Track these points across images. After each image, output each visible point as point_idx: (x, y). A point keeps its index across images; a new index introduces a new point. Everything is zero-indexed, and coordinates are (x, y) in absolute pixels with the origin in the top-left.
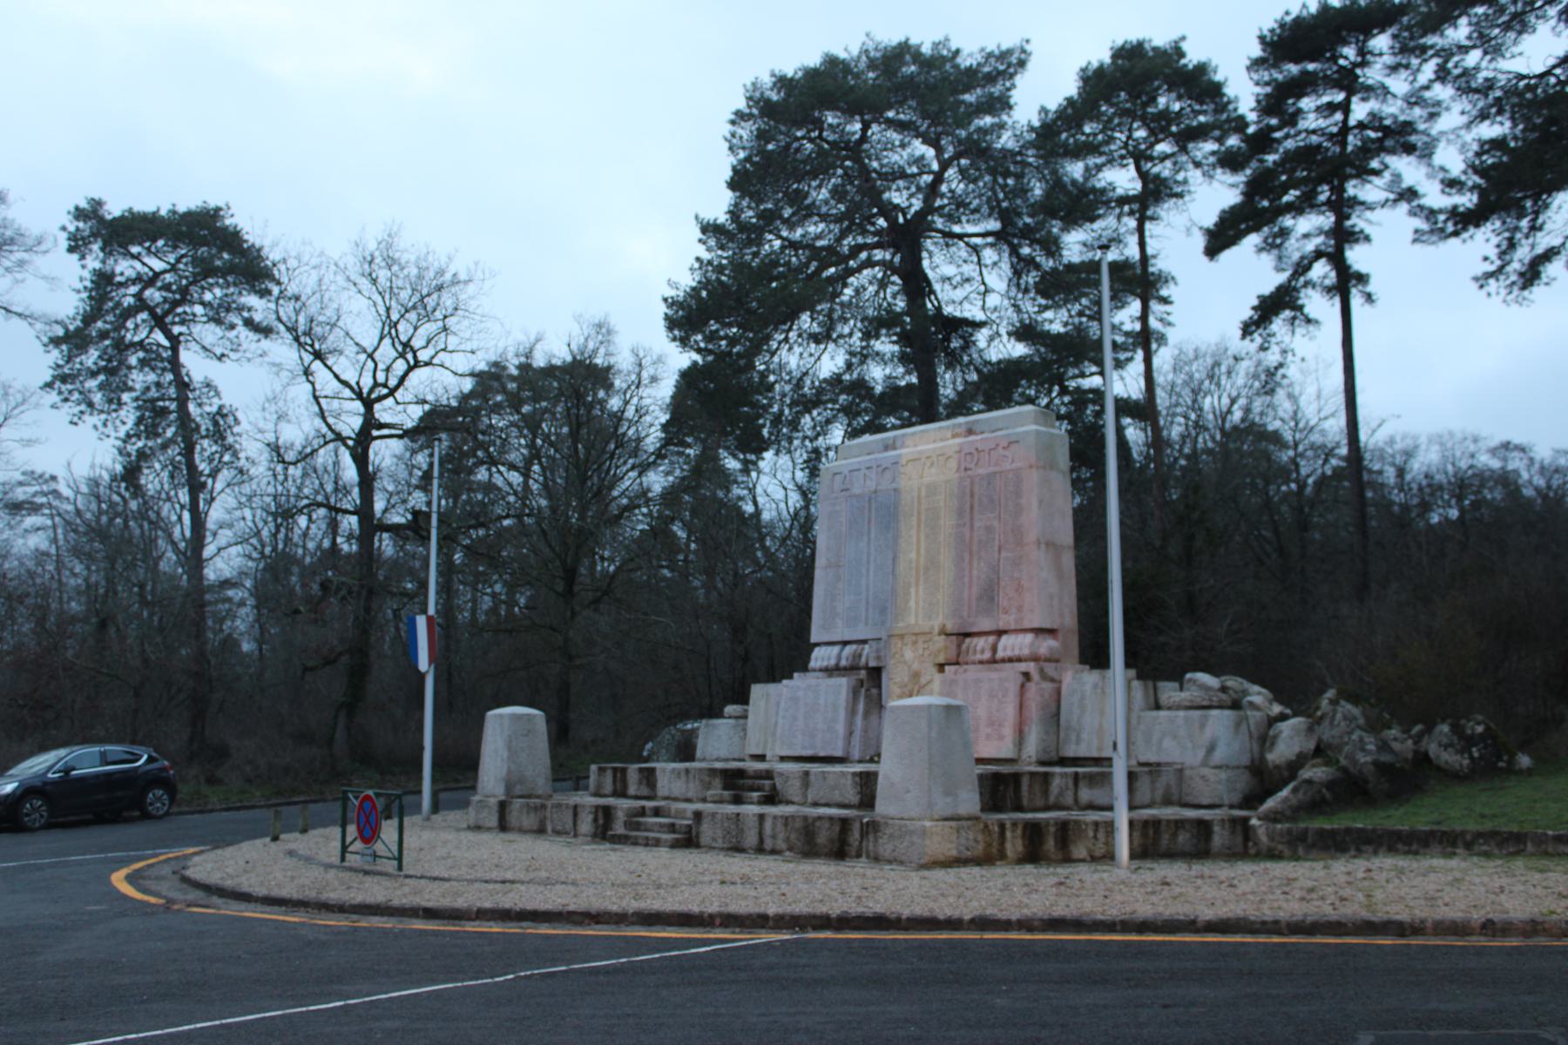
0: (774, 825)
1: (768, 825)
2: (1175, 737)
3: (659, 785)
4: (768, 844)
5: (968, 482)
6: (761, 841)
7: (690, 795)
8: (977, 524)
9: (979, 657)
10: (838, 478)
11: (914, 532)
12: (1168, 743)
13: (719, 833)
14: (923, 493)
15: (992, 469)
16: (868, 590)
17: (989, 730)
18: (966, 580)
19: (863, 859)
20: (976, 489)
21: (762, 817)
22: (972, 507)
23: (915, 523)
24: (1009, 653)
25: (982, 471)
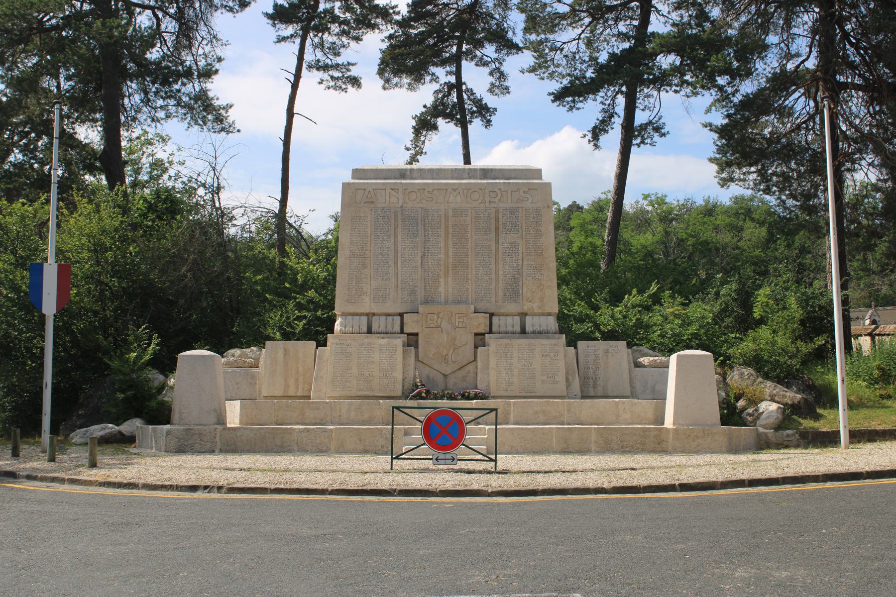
5: (493, 210)
8: (501, 240)
9: (510, 329)
10: (361, 192)
11: (442, 239)
14: (450, 214)
15: (516, 205)
18: (493, 276)
20: (501, 216)
22: (497, 228)
23: (443, 234)
25: (502, 205)
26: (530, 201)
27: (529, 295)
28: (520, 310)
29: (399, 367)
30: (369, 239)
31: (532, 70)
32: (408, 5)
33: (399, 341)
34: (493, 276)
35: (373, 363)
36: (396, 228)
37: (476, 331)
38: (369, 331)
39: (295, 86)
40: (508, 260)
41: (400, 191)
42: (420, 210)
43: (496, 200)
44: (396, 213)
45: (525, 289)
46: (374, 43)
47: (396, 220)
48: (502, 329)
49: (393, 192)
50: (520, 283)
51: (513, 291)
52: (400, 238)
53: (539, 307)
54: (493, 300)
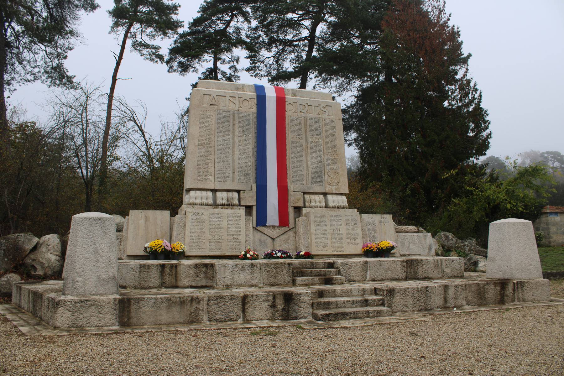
0: (456, 291)
1: (451, 292)
2: (414, 244)
3: (218, 276)
4: (451, 303)
5: (303, 118)
6: (445, 300)
7: (255, 282)
8: (310, 140)
9: (318, 204)
12: (412, 246)
13: (410, 301)
16: (234, 161)
17: (349, 241)
18: (304, 166)
19: (516, 302)
20: (308, 123)
21: (446, 287)
22: (306, 131)
24: (336, 204)
25: (309, 115)
26: (327, 113)
27: (329, 181)
28: (323, 191)
29: (243, 232)
30: (213, 132)
31: (248, 70)
32: (189, 23)
33: (242, 211)
34: (304, 166)
35: (222, 228)
36: (234, 125)
37: (296, 205)
38: (215, 205)
39: (118, 64)
40: (314, 154)
41: (237, 98)
42: (251, 114)
43: (305, 111)
44: (234, 114)
45: (326, 176)
46: (165, 43)
47: (234, 119)
48: (313, 204)
49: (231, 99)
50: (323, 172)
51: (318, 177)
52: (237, 133)
53: (336, 189)
54: (305, 183)
